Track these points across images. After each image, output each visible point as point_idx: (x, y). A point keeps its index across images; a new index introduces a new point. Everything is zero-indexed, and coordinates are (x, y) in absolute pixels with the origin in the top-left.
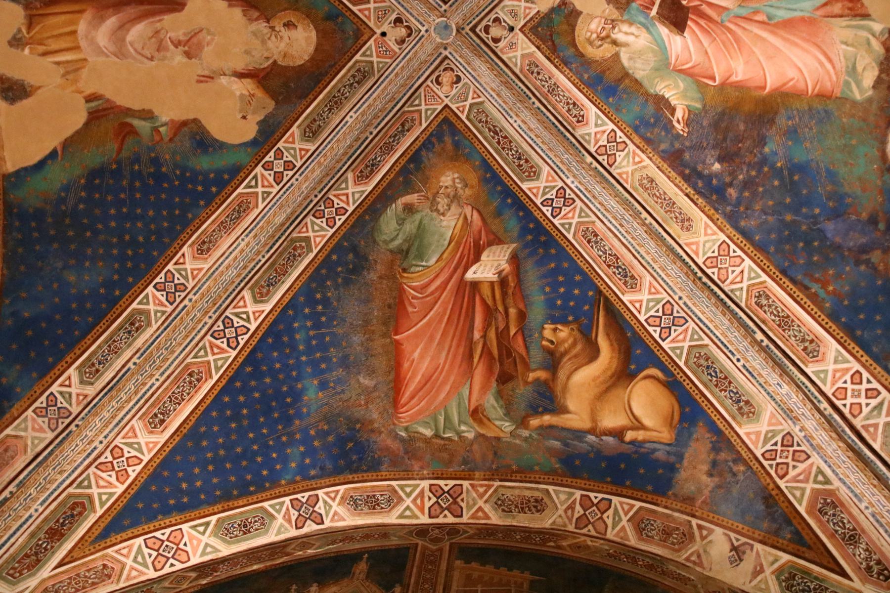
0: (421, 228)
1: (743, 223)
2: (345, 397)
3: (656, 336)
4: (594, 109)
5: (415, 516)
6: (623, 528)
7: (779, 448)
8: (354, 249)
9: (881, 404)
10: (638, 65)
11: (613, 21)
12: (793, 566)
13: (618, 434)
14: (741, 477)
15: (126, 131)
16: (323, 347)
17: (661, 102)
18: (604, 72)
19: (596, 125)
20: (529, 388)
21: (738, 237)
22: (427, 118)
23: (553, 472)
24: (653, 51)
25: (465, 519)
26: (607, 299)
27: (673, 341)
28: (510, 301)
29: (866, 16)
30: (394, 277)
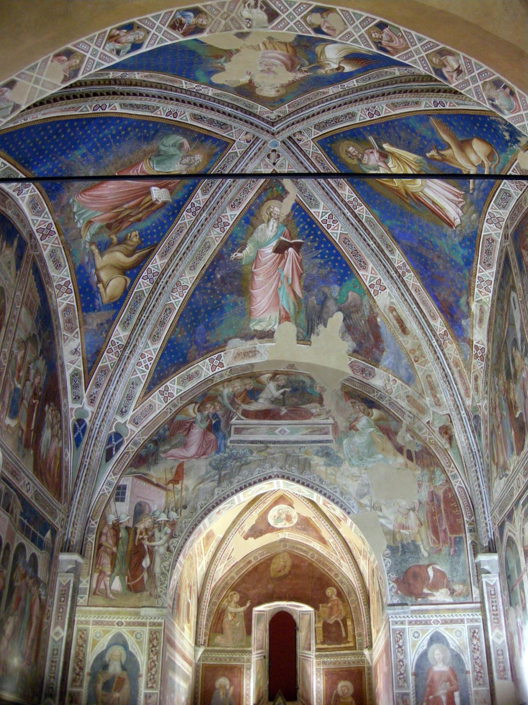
0: (171, 157)
1: (197, 292)
2: (81, 167)
3: (144, 275)
4: (238, 213)
5: (34, 224)
6: (63, 303)
7: (117, 345)
8: (157, 131)
9: (145, 372)
10: (259, 234)
11: (278, 219)
12: (80, 373)
13: (99, 281)
14: (101, 337)
15: (218, 57)
16: (103, 145)
17: (243, 247)
18: (255, 216)
19: (231, 215)
20: (108, 238)
21: (191, 292)
22: (228, 135)
23: (74, 265)
24: (266, 240)
25: (41, 242)
26: (154, 249)
27: (143, 282)
28: (145, 212)
29: (280, 323)
30: (145, 155)
